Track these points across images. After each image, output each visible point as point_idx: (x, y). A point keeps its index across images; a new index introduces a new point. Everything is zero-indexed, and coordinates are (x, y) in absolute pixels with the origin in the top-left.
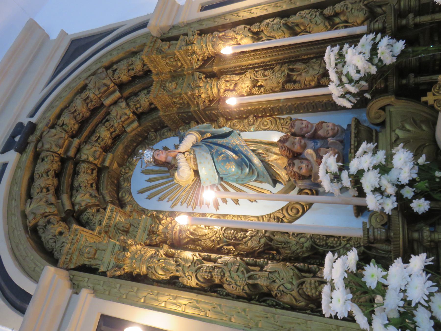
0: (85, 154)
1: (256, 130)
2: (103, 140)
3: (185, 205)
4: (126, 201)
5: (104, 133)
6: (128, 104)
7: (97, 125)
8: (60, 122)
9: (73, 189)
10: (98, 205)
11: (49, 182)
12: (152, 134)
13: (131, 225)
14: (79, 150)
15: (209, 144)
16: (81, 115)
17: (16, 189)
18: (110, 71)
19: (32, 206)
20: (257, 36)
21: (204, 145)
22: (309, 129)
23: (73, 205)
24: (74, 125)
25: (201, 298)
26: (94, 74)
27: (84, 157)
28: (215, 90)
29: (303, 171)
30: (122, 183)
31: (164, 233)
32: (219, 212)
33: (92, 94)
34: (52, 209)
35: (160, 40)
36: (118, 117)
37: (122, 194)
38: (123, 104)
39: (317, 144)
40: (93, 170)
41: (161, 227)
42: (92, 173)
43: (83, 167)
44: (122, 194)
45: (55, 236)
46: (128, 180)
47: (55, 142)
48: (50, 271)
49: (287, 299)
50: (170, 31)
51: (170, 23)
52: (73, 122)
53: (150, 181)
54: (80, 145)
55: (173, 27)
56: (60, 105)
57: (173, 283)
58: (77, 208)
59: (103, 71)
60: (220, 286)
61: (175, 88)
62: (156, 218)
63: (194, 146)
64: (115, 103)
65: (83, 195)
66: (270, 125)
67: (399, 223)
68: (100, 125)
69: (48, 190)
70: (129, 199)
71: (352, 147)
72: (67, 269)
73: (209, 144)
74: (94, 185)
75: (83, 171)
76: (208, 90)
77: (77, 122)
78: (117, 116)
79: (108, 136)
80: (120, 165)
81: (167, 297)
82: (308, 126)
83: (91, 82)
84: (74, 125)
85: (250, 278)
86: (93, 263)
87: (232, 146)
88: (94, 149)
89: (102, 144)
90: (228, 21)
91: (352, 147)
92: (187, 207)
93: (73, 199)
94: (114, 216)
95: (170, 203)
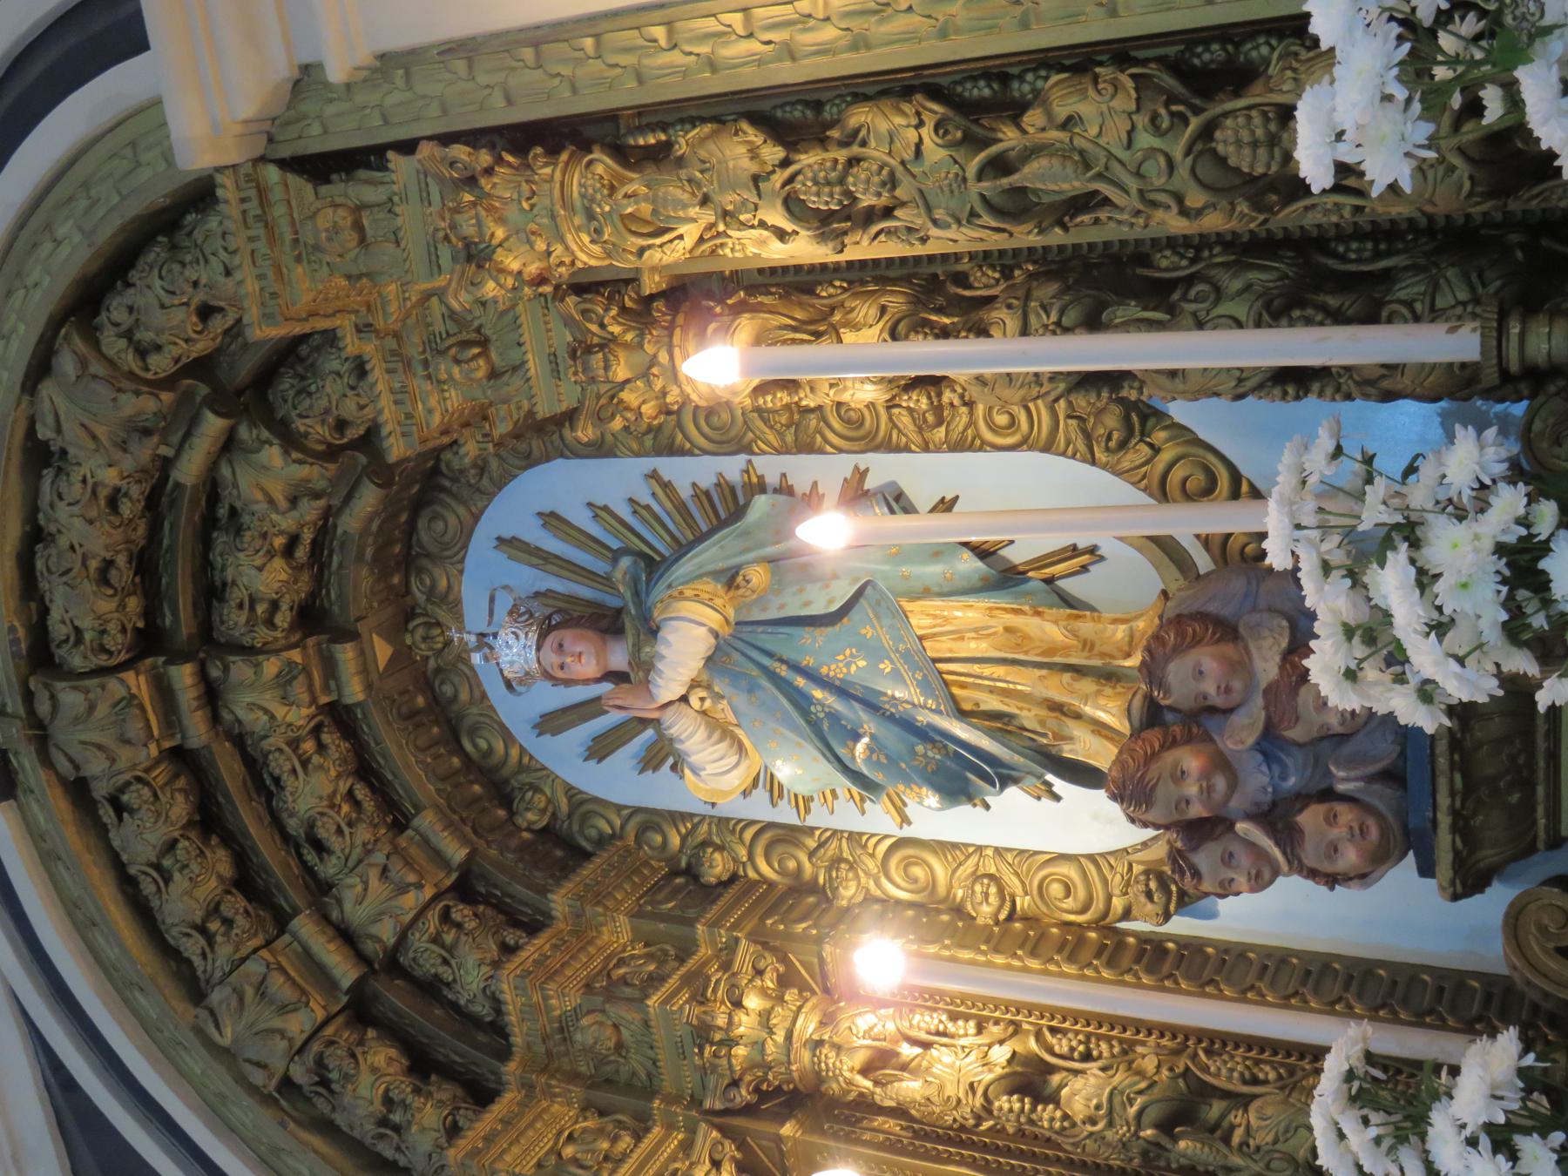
1: (958, 446)
2: (275, 606)
4: (506, 772)
6: (291, 441)
10: (436, 898)
11: (210, 887)
13: (616, 1026)
15: (783, 671)
16: (121, 560)
17: (112, 953)
18: (113, 344)
19: (228, 1031)
21: (765, 683)
22: (1235, 697)
23: (347, 936)
24: (122, 606)
26: (40, 367)
30: (448, 690)
32: (907, 832)
35: (272, 173)
36: (283, 503)
37: (475, 746)
38: (273, 455)
39: (1284, 778)
40: (316, 731)
41: (740, 1051)
42: (321, 748)
44: (475, 746)
45: (383, 1122)
50: (304, 107)
51: (282, 70)
52: (106, 605)
54: (203, 675)
55: (307, 78)
59: (83, 363)
61: (494, 374)
65: (359, 888)
66: (1024, 426)
69: (228, 923)
70: (514, 752)
71: (1444, 801)
73: (783, 671)
74: (361, 792)
75: (287, 767)
77: (123, 594)
78: (271, 502)
79: (284, 577)
82: (1228, 690)
83: (65, 426)
84: (122, 606)
87: (895, 706)
88: (271, 667)
89: (283, 619)
91: (1444, 801)
92: (774, 804)
93: (335, 915)
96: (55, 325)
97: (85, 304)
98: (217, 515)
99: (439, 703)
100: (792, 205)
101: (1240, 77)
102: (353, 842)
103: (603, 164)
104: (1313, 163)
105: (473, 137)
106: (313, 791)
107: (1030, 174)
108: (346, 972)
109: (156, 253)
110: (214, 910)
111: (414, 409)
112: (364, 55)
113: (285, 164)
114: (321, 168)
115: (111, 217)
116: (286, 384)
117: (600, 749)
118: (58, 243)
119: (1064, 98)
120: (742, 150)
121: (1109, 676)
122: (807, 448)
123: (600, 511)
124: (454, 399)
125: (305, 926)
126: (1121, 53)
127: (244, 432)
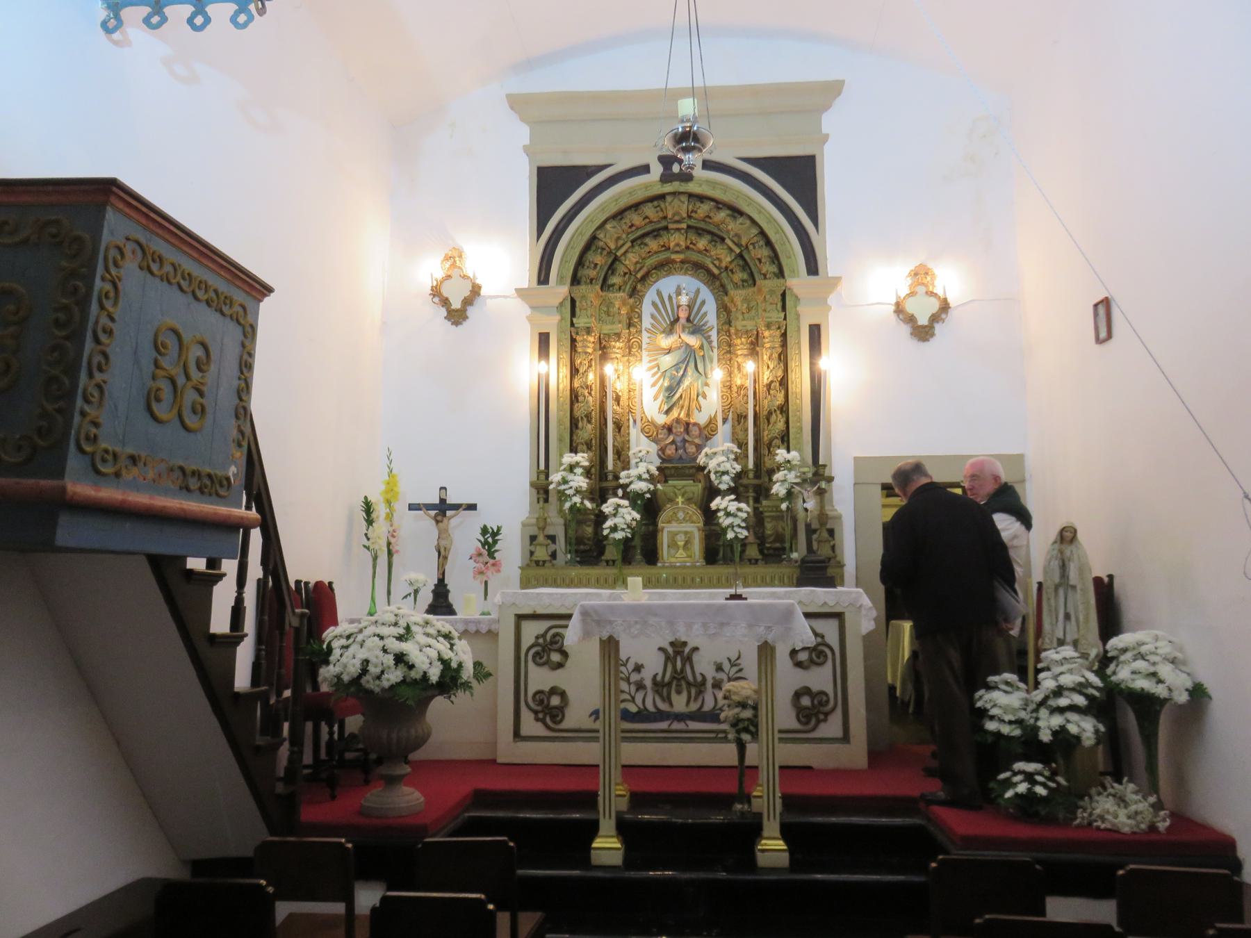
5: (702, 243)
7: (709, 232)
8: (698, 204)
9: (639, 240)
12: (717, 283)
14: (678, 230)
20: (769, 386)
27: (672, 238)
28: (739, 352)
33: (734, 226)
34: (613, 246)
38: (729, 259)
46: (669, 273)
47: (676, 207)
48: (564, 290)
53: (670, 298)
57: (574, 371)
63: (687, 345)
64: (731, 250)
67: (614, 484)
68: (709, 237)
76: (741, 344)
80: (682, 262)
81: (565, 371)
86: (577, 310)
94: (617, 298)
98: (718, 238)
101: (783, 441)
103: (780, 350)
104: (778, 451)
106: (653, 244)
108: (619, 254)
110: (632, 225)
111: (738, 295)
114: (783, 295)
116: (741, 263)
117: (654, 304)
119: (783, 420)
120: (780, 373)
121: (688, 415)
123: (705, 314)
124: (739, 303)
126: (788, 427)
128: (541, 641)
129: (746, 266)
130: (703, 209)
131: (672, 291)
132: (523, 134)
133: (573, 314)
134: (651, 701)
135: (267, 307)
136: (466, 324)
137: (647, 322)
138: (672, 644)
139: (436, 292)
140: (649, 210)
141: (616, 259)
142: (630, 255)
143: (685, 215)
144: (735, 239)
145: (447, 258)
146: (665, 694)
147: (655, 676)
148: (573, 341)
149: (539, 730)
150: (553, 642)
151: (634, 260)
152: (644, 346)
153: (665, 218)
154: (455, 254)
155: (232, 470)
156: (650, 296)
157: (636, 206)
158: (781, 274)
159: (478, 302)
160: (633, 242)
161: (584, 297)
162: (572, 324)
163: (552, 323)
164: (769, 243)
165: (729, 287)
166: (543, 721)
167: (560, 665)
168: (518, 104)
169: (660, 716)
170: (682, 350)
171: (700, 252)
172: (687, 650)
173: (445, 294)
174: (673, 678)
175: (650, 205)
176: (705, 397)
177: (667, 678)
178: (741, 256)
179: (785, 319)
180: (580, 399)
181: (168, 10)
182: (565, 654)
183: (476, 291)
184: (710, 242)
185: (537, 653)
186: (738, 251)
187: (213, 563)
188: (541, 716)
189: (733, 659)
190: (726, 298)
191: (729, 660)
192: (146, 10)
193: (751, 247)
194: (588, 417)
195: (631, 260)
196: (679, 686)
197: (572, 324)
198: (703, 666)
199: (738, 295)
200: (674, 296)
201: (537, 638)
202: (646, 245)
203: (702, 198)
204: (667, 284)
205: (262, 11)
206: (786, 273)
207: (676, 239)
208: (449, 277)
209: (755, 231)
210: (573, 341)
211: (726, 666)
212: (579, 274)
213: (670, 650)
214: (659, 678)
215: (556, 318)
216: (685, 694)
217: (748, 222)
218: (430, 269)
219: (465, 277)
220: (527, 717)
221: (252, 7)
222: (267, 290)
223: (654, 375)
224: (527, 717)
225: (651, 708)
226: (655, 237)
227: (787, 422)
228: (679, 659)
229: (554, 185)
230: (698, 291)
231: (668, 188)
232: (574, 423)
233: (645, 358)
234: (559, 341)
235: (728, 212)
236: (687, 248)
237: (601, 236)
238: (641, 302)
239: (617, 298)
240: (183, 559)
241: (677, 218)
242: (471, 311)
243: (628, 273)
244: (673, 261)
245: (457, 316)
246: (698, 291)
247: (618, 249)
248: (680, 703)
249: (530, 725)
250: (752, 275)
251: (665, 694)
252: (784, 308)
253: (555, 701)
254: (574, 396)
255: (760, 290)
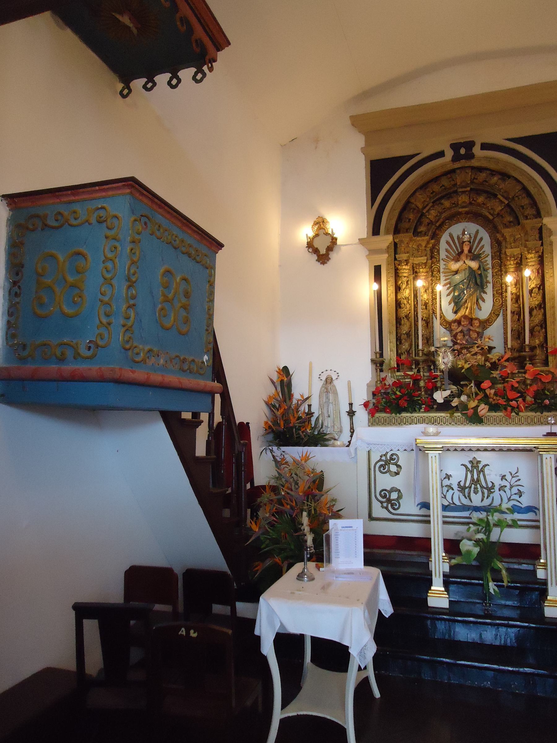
0: (462, 198)
1: (493, 295)
3: (444, 267)
20: (531, 292)
23: (428, 211)
25: (394, 302)
27: (460, 199)
29: (453, 327)
31: (420, 272)
34: (420, 207)
35: (541, 225)
38: (500, 208)
43: (454, 200)
46: (458, 222)
48: (390, 238)
49: (399, 331)
52: (481, 181)
53: (458, 237)
54: (467, 191)
56: (492, 166)
57: (398, 289)
58: (427, 214)
60: (400, 308)
62: (433, 254)
64: (501, 202)
68: (485, 195)
69: (432, 193)
72: (393, 239)
80: (467, 213)
81: (392, 289)
85: (403, 318)
86: (398, 250)
89: (473, 202)
90: (546, 271)
95: (445, 257)
96: (522, 184)
97: (525, 189)
99: (454, 218)
100: (534, 288)
102: (439, 208)
105: (543, 253)
106: (447, 203)
107: (535, 310)
109: (532, 202)
110: (433, 192)
112: (553, 240)
113: (541, 226)
114: (540, 230)
115: (536, 197)
116: (509, 210)
117: (448, 243)
118: (534, 188)
122: (493, 276)
123: (483, 246)
125: (431, 205)
127: (503, 205)
128: (384, 458)
129: (512, 212)
130: (482, 176)
131: (460, 233)
132: (359, 141)
133: (396, 253)
134: (458, 498)
135: (220, 256)
136: (330, 263)
137: (443, 254)
138: (471, 462)
139: (310, 245)
140: (445, 182)
141: (423, 215)
142: (432, 212)
143: (469, 182)
144: (505, 195)
145: (316, 223)
146: (467, 495)
147: (459, 482)
148: (396, 270)
149: (384, 514)
150: (391, 459)
151: (435, 215)
152: (441, 270)
153: (455, 185)
154: (320, 220)
155: (206, 358)
156: (445, 238)
157: (436, 179)
158: (538, 215)
159: (335, 248)
160: (433, 203)
161: (401, 241)
162: (395, 259)
163: (383, 259)
164: (529, 194)
165: (500, 227)
166: (387, 508)
167: (397, 474)
168: (358, 122)
169: (464, 508)
170: (467, 271)
171: (479, 205)
172: (480, 466)
173: (316, 246)
174: (471, 484)
175: (445, 177)
176: (484, 301)
177: (467, 484)
178: (508, 205)
179: (542, 245)
180: (403, 305)
181: (156, 79)
182: (399, 466)
183: (334, 240)
184: (486, 198)
185: (381, 466)
186: (506, 202)
187: (196, 415)
188: (385, 505)
189: (513, 473)
190: (498, 236)
191: (511, 474)
192: (144, 80)
193: (516, 199)
194: (407, 317)
195: (432, 214)
196: (476, 488)
197: (395, 259)
198: (492, 476)
199: (507, 232)
200: (461, 236)
201: (381, 456)
202: (442, 204)
203: (481, 169)
204: (456, 229)
205: (211, 69)
206: (542, 213)
207: (463, 199)
208: (317, 235)
209: (519, 187)
210: (396, 270)
211: (509, 477)
212: (399, 227)
213: (469, 466)
214: (462, 484)
215: (386, 256)
216: (480, 493)
217: (514, 182)
218: (306, 231)
219: (327, 234)
220: (376, 505)
221: (205, 68)
222: (220, 246)
223: (448, 289)
224: (376, 505)
225: (458, 503)
226: (448, 198)
227: (545, 315)
228: (475, 470)
229: (381, 172)
230: (477, 232)
231: (457, 165)
232: (398, 321)
233: (442, 278)
234: (387, 270)
235: (500, 177)
236: (471, 203)
237: (412, 200)
238: (438, 242)
239: (423, 240)
240: (179, 413)
241: (463, 184)
242: (333, 255)
243: (431, 223)
244: (460, 213)
245: (323, 259)
246: (477, 232)
247: (424, 208)
248: (476, 500)
249: (379, 511)
250: (517, 218)
251: (467, 495)
252: (541, 238)
253: (394, 496)
254: (398, 305)
255: (523, 228)
